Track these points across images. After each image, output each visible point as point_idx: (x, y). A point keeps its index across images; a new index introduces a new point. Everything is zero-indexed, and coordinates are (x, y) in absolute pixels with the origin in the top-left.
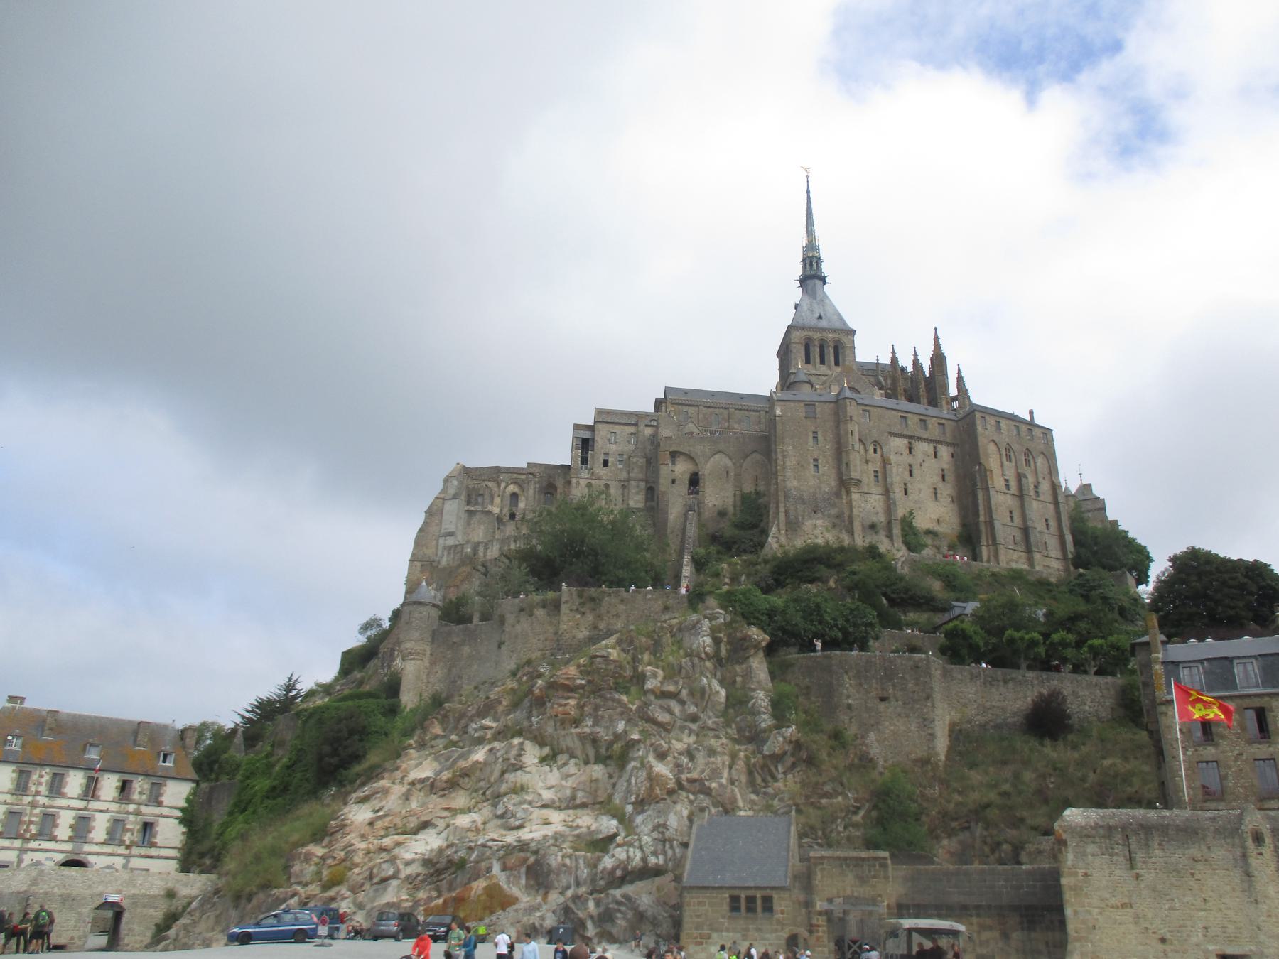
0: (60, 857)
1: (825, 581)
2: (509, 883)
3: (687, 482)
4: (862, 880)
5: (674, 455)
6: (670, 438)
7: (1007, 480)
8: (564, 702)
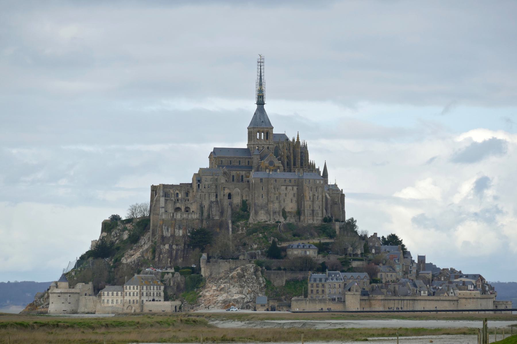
0: (152, 299)
1: (264, 233)
3: (228, 196)
4: (274, 303)
5: (224, 188)
7: (310, 197)
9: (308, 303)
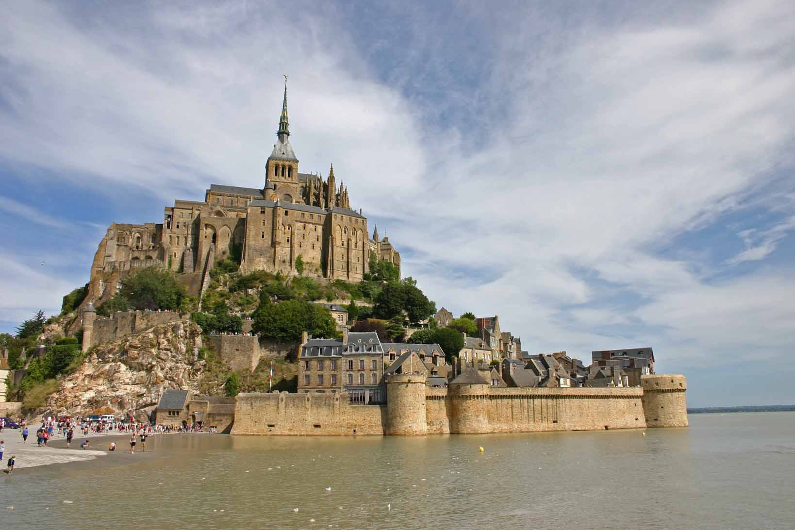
2: (112, 407)
6: (205, 218)
8: (133, 352)
9: (282, 405)
